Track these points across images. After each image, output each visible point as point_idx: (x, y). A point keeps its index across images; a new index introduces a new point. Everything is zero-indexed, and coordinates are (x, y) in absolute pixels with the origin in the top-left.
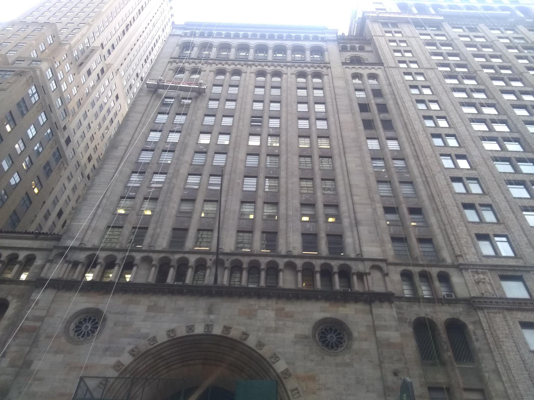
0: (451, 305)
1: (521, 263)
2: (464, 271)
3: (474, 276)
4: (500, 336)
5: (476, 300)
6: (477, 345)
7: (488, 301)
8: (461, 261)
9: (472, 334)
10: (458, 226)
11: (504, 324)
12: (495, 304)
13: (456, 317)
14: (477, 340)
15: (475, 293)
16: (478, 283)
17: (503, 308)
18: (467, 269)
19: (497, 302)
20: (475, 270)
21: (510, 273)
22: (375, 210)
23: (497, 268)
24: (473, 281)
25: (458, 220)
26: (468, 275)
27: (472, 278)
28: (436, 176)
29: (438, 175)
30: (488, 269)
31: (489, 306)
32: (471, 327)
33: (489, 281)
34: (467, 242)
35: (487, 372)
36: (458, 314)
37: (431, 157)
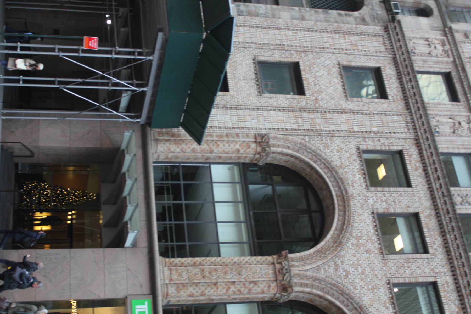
2: (440, 32)
3: (436, 39)
4: (353, 38)
5: (396, 24)
6: (334, 13)
7: (400, 36)
8: (459, 37)
9: (347, 12)
11: (371, 49)
12: (398, 45)
14: (340, 14)
15: (408, 34)
16: (427, 40)
17: (395, 54)
18: (445, 35)
19: (401, 47)
20: (447, 44)
21: (458, 86)
23: (461, 72)
24: (428, 36)
26: (436, 36)
27: (434, 37)
30: (454, 61)
31: (393, 39)
32: (356, 13)
33: (434, 52)
35: (300, 10)
36: (370, 7)
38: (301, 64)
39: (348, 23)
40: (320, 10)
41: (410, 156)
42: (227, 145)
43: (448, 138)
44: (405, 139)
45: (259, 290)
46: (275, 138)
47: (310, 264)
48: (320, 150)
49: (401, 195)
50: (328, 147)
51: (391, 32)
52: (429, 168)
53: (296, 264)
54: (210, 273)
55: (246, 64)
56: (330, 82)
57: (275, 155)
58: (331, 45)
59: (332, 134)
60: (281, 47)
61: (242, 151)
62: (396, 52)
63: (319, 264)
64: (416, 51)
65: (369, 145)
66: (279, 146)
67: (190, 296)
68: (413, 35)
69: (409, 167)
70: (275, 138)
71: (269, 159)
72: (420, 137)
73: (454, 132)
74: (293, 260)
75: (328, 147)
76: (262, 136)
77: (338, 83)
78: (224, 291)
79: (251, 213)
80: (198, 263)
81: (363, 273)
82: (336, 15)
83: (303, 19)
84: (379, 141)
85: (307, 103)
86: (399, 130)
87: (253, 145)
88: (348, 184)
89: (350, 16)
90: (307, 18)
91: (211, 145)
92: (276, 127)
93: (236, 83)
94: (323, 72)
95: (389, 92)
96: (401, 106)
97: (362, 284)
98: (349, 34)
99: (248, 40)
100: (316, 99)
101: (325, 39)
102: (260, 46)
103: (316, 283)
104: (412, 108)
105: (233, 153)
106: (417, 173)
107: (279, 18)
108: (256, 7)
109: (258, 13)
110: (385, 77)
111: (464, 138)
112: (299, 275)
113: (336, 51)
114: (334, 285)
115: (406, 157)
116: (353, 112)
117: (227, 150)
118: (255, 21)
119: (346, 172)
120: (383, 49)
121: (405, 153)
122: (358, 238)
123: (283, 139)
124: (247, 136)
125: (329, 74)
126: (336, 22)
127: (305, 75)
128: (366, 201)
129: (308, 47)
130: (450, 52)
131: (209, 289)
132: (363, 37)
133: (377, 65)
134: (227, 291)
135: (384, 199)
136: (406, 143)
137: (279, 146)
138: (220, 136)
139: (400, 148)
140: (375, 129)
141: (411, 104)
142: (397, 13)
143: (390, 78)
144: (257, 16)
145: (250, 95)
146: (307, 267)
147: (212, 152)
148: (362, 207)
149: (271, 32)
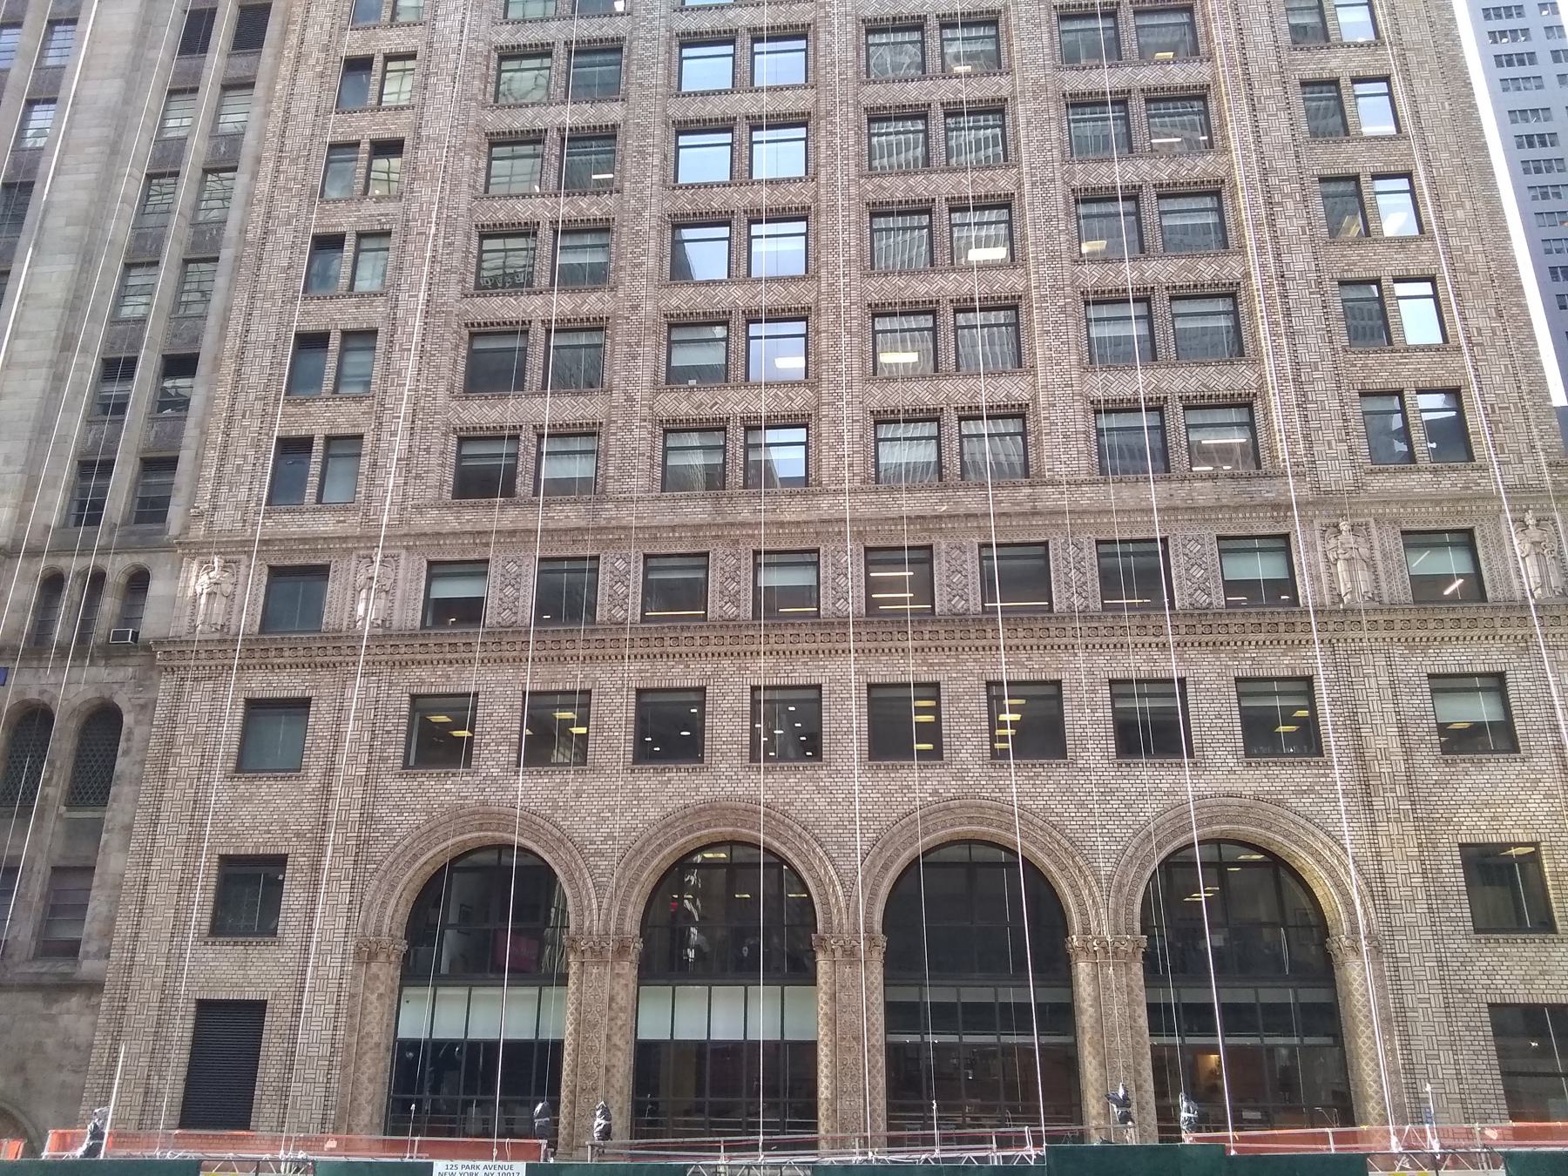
0: (112, 662)
1: (352, 524)
6: (121, 764)
8: (199, 531)
9: (122, 738)
10: (244, 416)
11: (206, 707)
13: (107, 695)
14: (126, 753)
15: (180, 628)
22: (58, 379)
25: (252, 397)
28: (271, 238)
29: (281, 231)
32: (128, 719)
34: (239, 469)
35: (108, 831)
37: (294, 161)
38: (223, 851)
39: (148, 741)
40: (113, 790)
41: (423, 682)
42: (369, 1018)
43: (397, 604)
44: (390, 683)
45: (622, 994)
46: (365, 925)
47: (590, 900)
48: (396, 845)
49: (491, 715)
50: (393, 830)
51: (176, 663)
52: (449, 656)
53: (587, 924)
54: (588, 1078)
55: (214, 960)
56: (269, 801)
57: (394, 926)
58: (191, 786)
59: (367, 818)
60: (185, 884)
61: (382, 990)
62: (217, 662)
63: (590, 885)
64: (220, 623)
65: (395, 752)
66: (380, 920)
67: (621, 1113)
68: (187, 619)
69: (441, 690)
70: (365, 925)
71: (399, 934)
72: (390, 657)
73: (387, 592)
74: (580, 928)
75: (393, 830)
76: (358, 951)
77: (269, 787)
78: (619, 1054)
79: (492, 976)
80: (571, 1097)
81: (612, 811)
82: (127, 759)
83: (128, 828)
84: (388, 732)
85: (304, 854)
86: (373, 692)
87: (374, 967)
88: (462, 806)
89: (130, 732)
90: (127, 819)
91: (366, 1048)
92: (342, 922)
93: (250, 984)
94: (244, 812)
95: (296, 694)
96: (326, 676)
97: (629, 815)
98: (170, 743)
99: (164, 950)
100: (297, 835)
101: (178, 795)
102: (179, 927)
103: (620, 893)
104: (334, 659)
105: (383, 1005)
106: (455, 677)
107: (122, 876)
108: (93, 919)
109: (107, 917)
110: (267, 695)
111: (400, 576)
112: (607, 922)
113: (205, 778)
114: (627, 865)
115: (424, 690)
116: (330, 770)
117: (378, 1017)
118: (123, 926)
119: (441, 806)
120: (210, 685)
121: (415, 690)
122: (555, 808)
123: (367, 911)
124: (354, 978)
125: (250, 800)
126: (143, 762)
127: (248, 849)
128: (495, 780)
129: (190, 833)
130: (228, 557)
131: (614, 1081)
132: (179, 719)
133: (241, 702)
134: (620, 1049)
135: (493, 747)
136: (398, 684)
137: (380, 920)
138: (351, 1029)
139: (406, 698)
140: (366, 736)
141: (326, 659)
142: (135, 635)
143: (270, 684)
144: (113, 920)
145: (277, 960)
146: (595, 906)
147: (378, 1045)
148: (505, 789)
149: (151, 899)
